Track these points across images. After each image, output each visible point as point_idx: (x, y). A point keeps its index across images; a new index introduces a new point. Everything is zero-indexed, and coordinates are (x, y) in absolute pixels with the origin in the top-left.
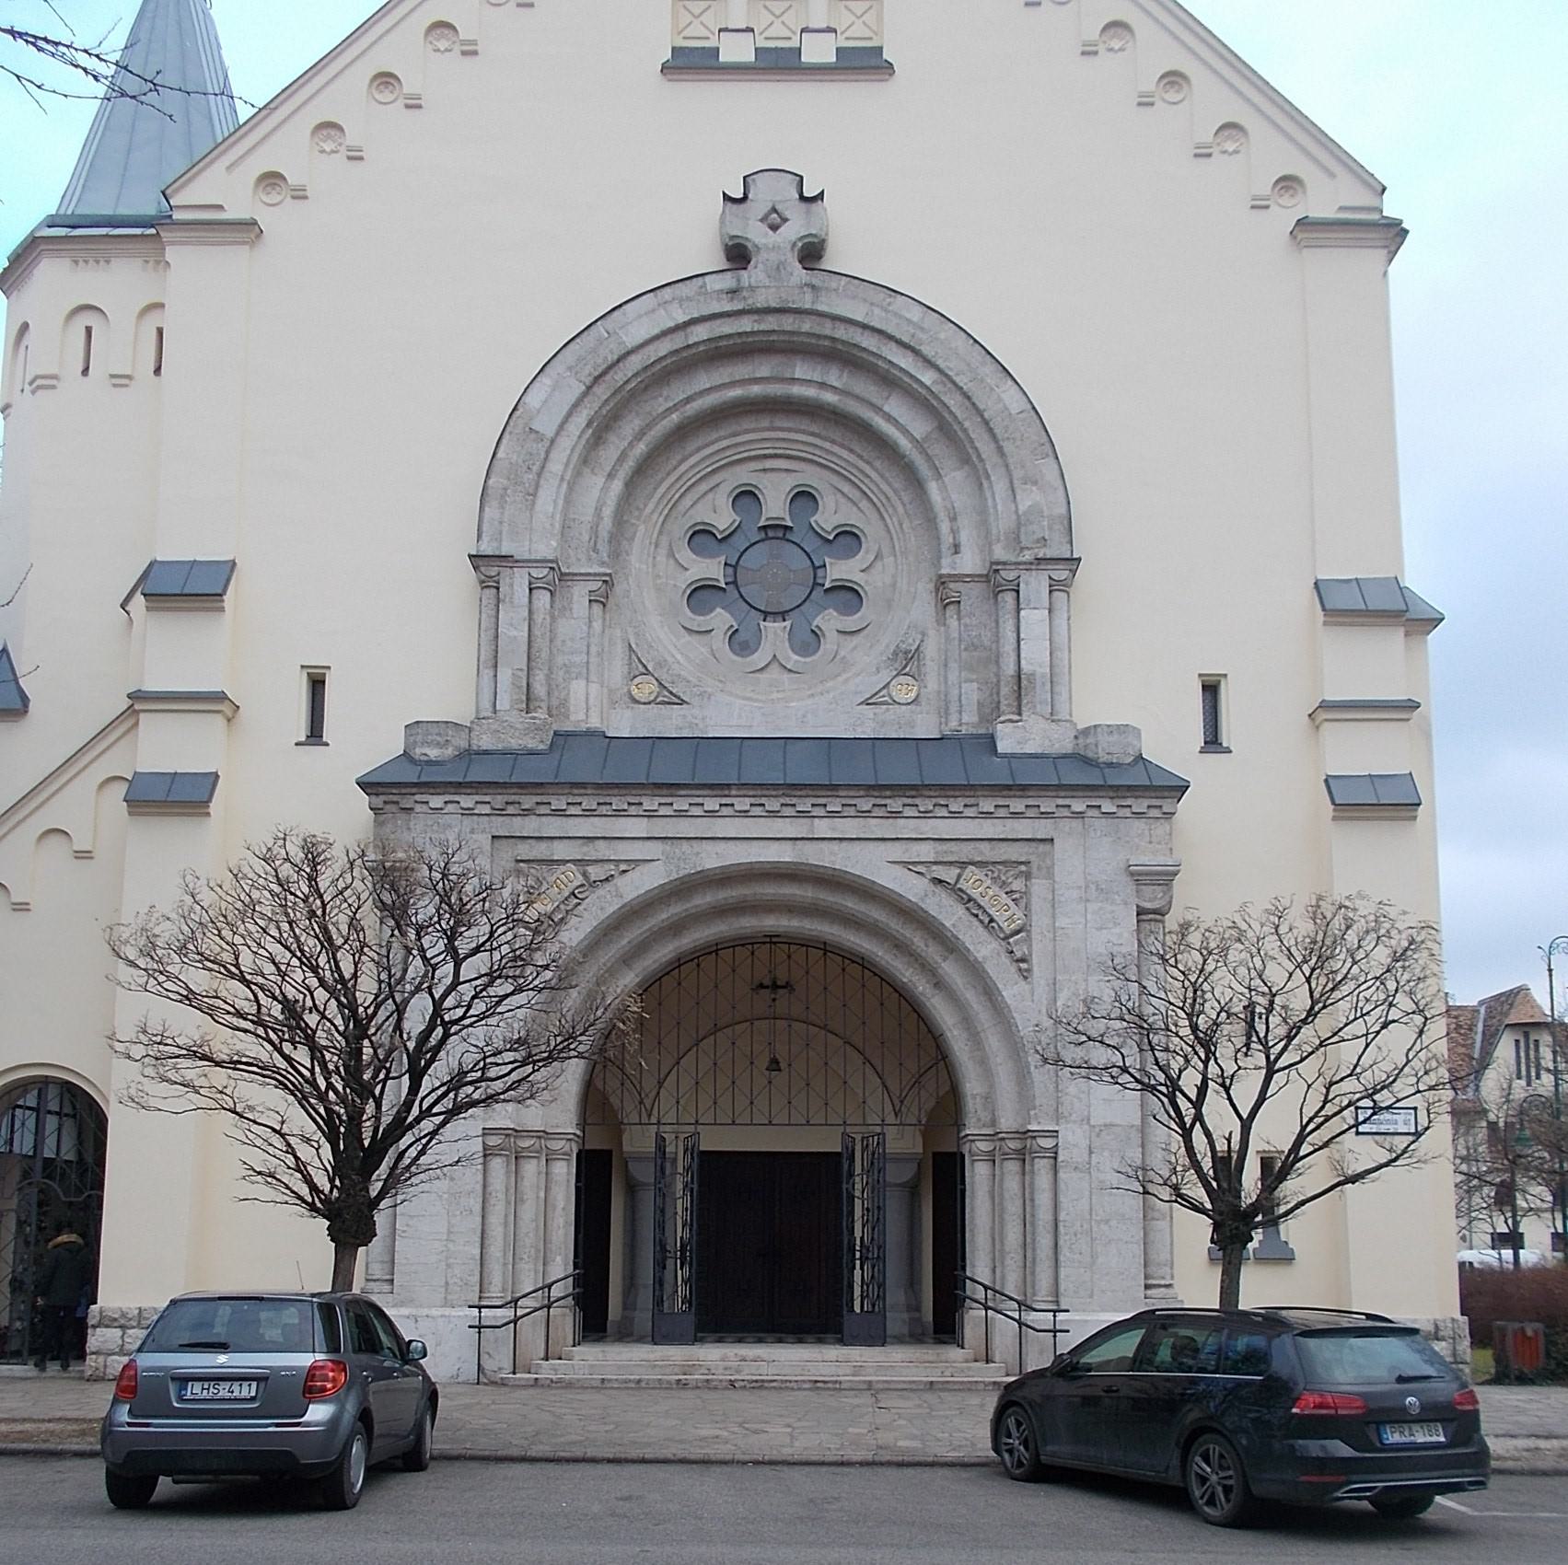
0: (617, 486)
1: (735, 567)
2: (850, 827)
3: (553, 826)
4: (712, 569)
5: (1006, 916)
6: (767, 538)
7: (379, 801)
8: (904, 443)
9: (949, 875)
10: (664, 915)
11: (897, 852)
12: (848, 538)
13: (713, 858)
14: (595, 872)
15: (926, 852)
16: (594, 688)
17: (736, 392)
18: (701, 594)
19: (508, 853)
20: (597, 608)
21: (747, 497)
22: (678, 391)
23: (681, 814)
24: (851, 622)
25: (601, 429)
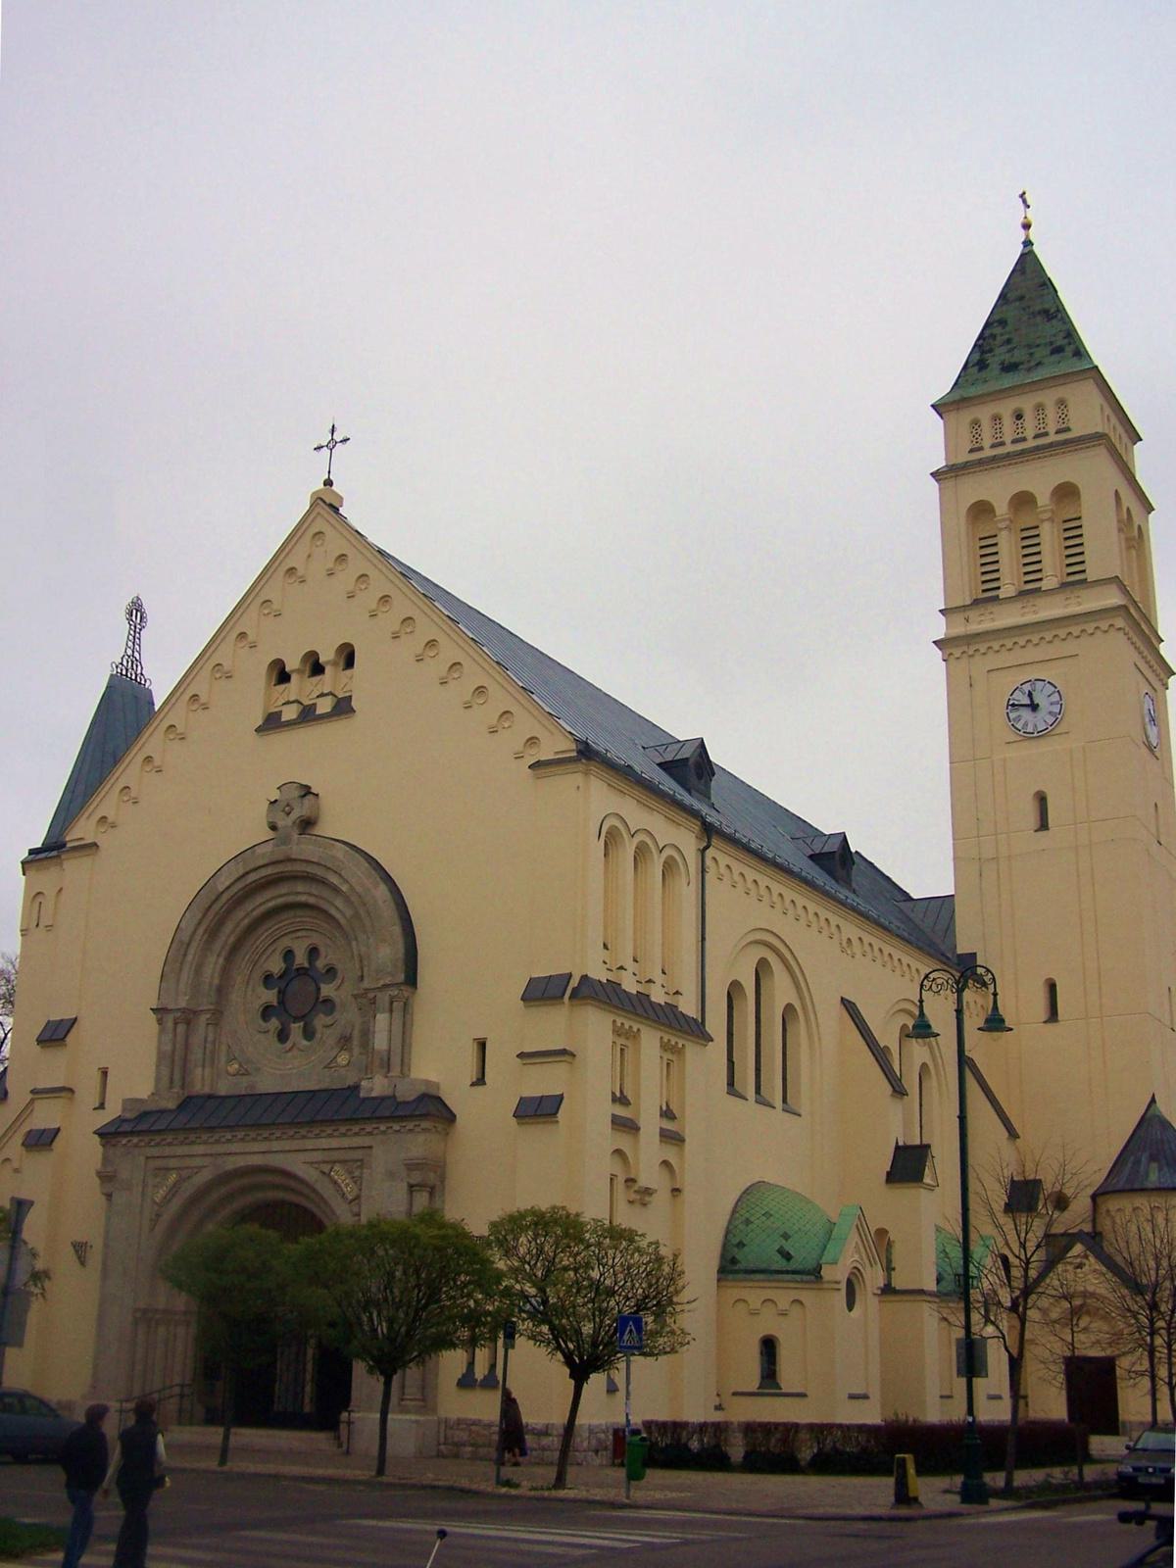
0: (221, 960)
1: (284, 993)
2: (286, 1145)
3: (167, 1151)
4: (270, 996)
5: (350, 1190)
6: (299, 975)
7: (104, 1141)
8: (343, 921)
9: (326, 1168)
10: (215, 1196)
11: (302, 1156)
12: (331, 971)
13: (232, 1163)
14: (185, 1173)
15: (318, 1156)
16: (207, 1071)
17: (271, 904)
18: (267, 1012)
19: (153, 1164)
20: (210, 1028)
21: (289, 955)
22: (249, 906)
23: (217, 1142)
24: (328, 1020)
25: (213, 933)
